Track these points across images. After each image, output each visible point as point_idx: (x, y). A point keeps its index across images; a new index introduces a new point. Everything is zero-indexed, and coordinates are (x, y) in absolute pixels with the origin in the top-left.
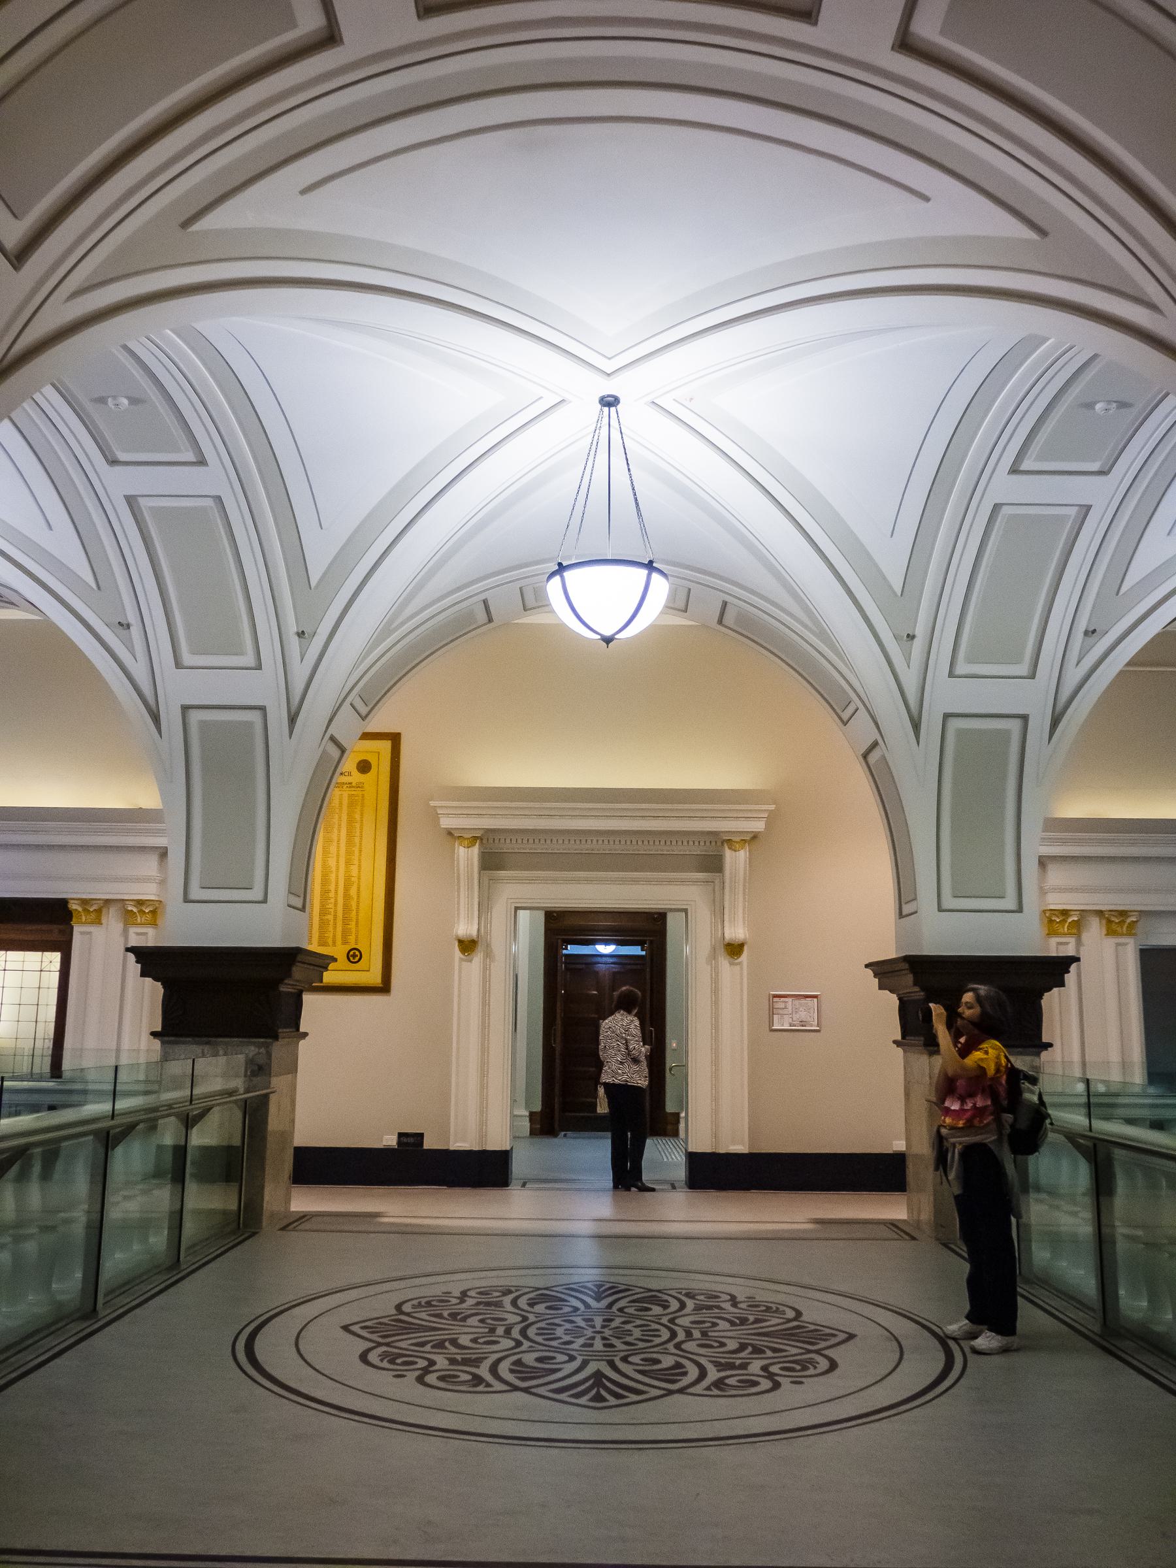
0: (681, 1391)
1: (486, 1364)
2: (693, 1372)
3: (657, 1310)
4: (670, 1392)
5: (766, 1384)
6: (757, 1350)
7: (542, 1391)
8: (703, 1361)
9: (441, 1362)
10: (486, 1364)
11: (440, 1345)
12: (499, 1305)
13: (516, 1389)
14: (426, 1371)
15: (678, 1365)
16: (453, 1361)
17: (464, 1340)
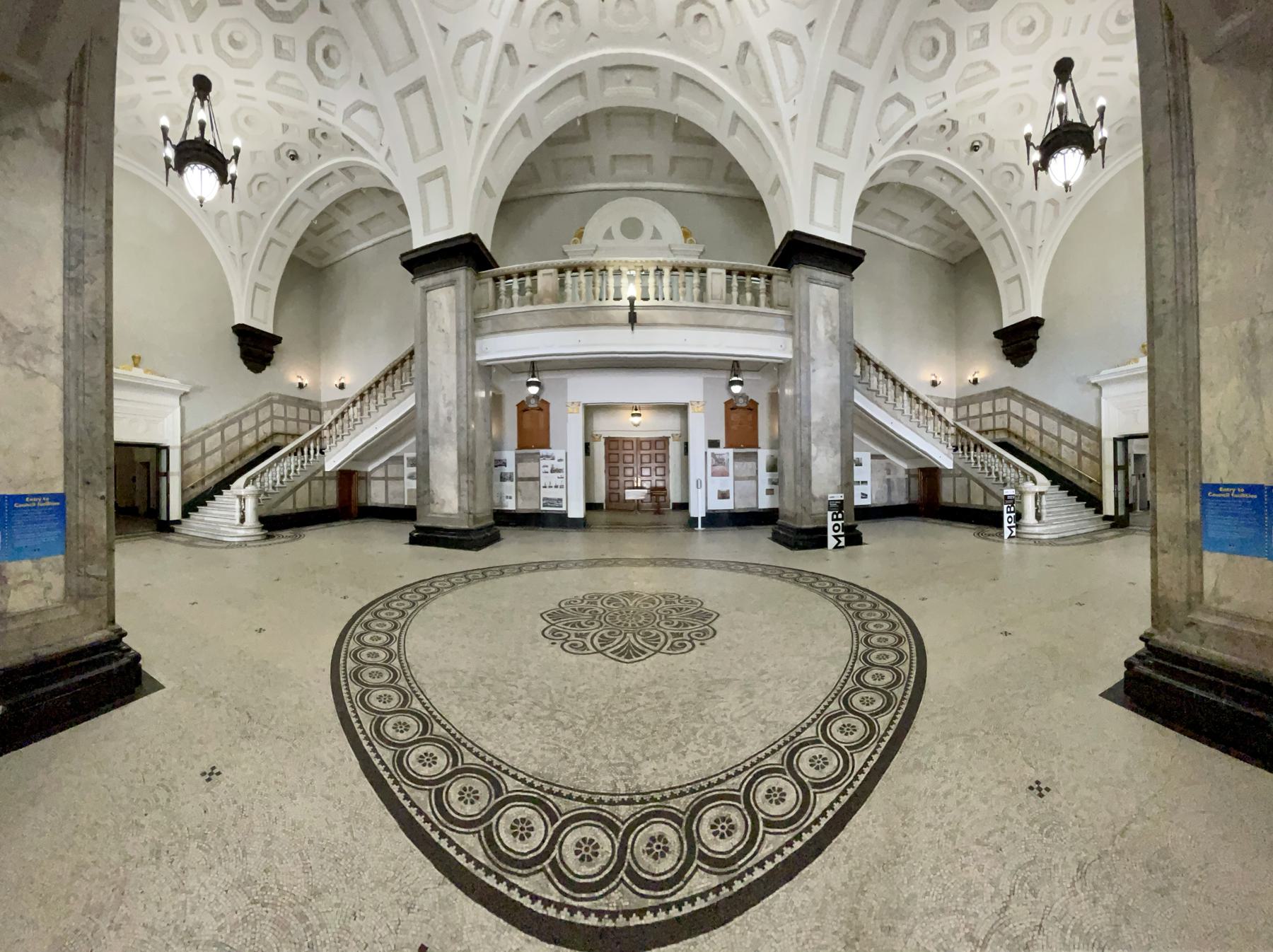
0: (659, 651)
1: (589, 637)
2: (662, 638)
3: (651, 606)
4: (656, 652)
5: (689, 645)
6: (686, 625)
7: (608, 652)
8: (668, 633)
9: (573, 637)
10: (589, 637)
11: (573, 626)
12: (595, 603)
13: (598, 651)
14: (566, 640)
15: (657, 636)
16: (577, 635)
17: (583, 623)
